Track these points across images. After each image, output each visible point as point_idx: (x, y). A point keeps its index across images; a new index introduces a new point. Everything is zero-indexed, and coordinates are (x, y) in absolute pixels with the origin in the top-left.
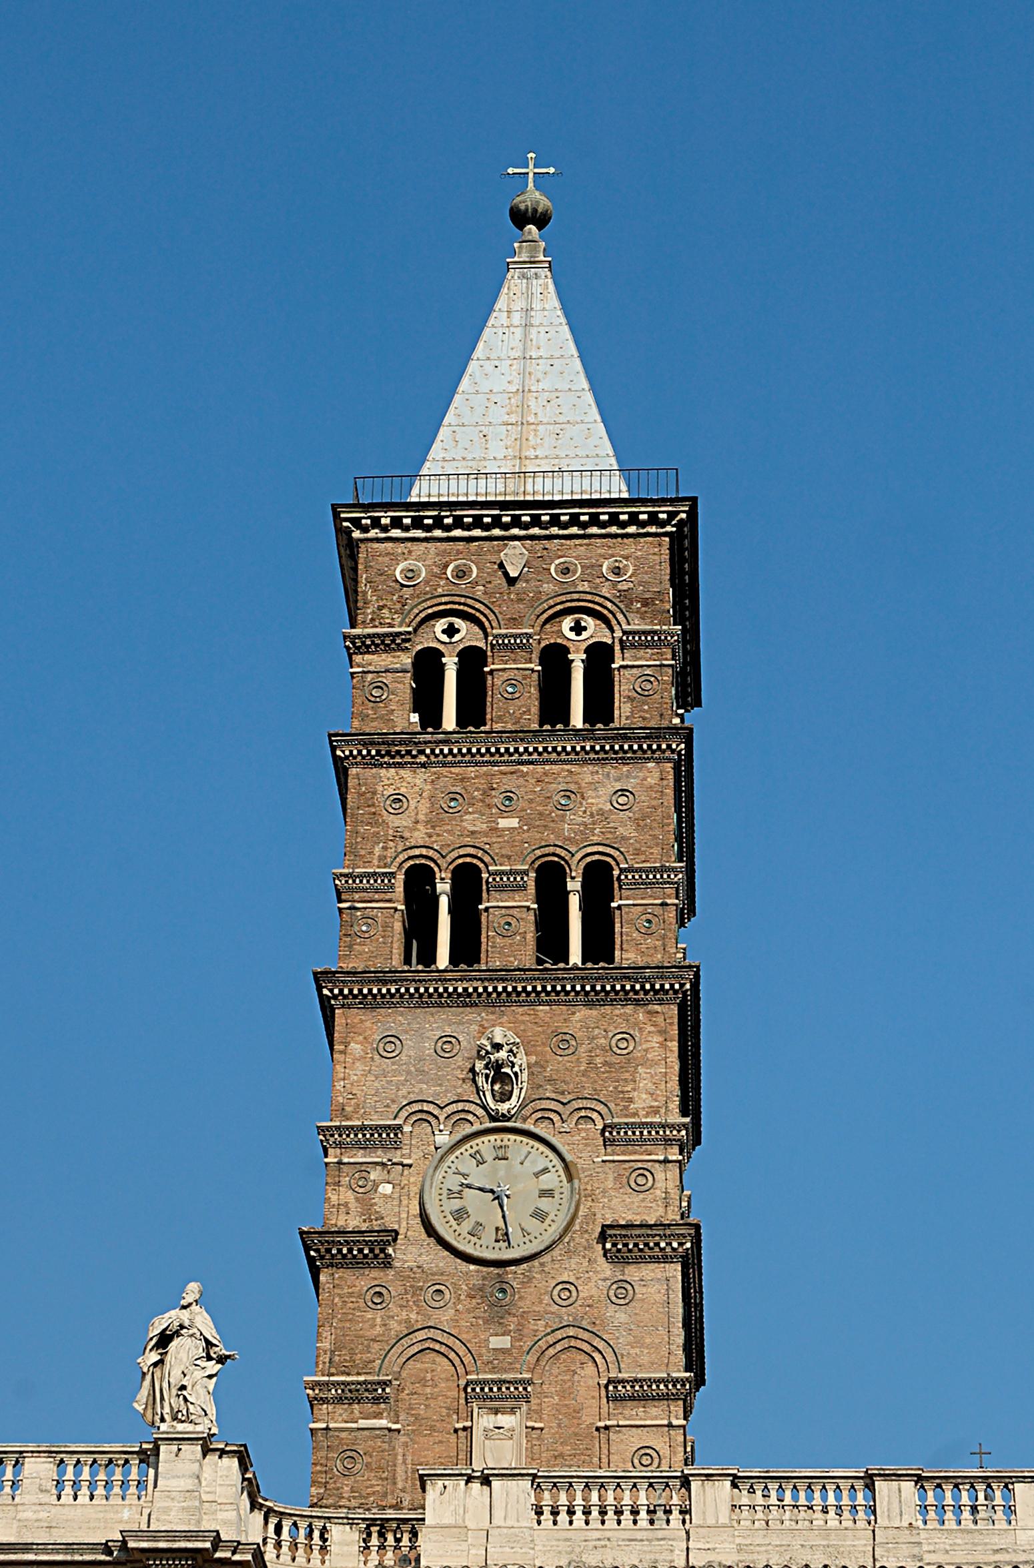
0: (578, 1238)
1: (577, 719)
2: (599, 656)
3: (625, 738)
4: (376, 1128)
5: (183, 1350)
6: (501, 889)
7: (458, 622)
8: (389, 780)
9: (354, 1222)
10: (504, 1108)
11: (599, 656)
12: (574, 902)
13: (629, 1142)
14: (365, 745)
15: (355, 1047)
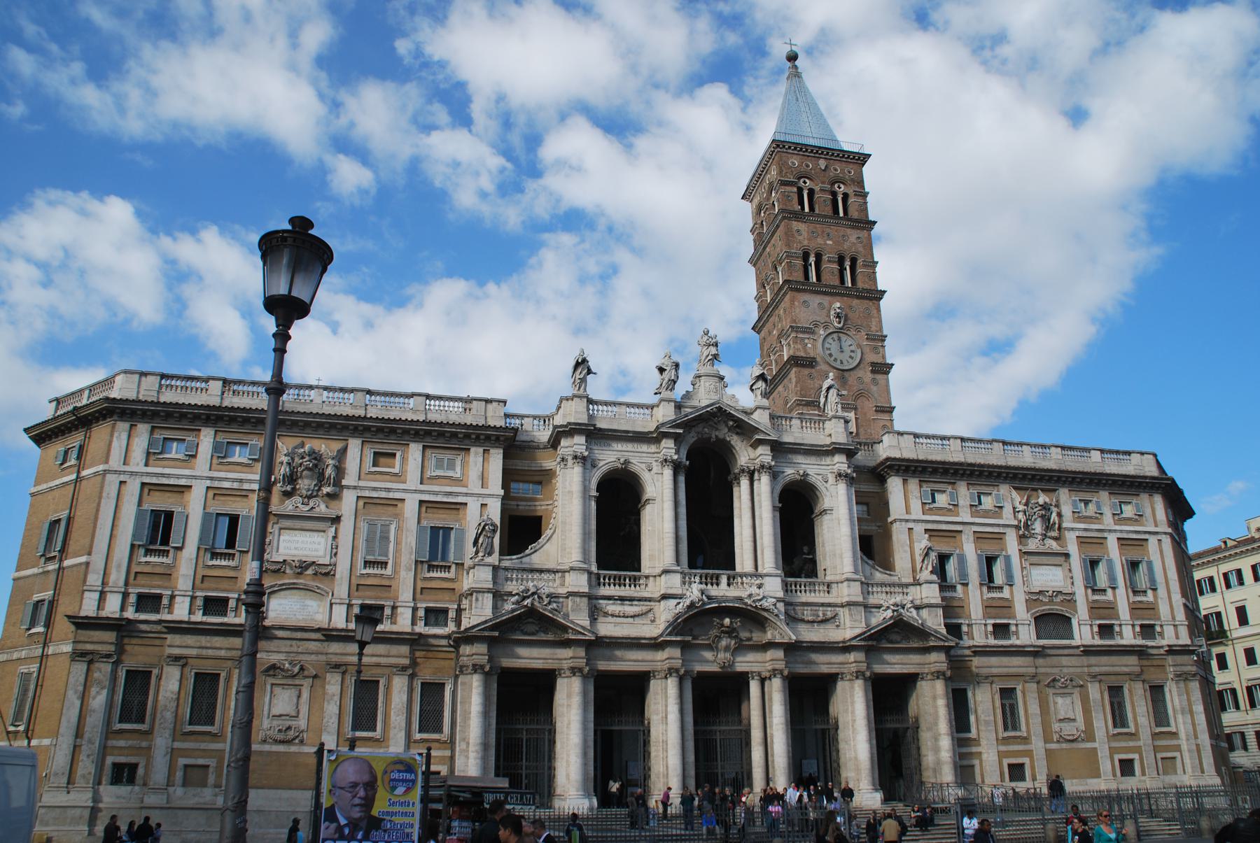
0: (862, 365)
1: (841, 214)
2: (846, 196)
3: (859, 222)
4: (806, 328)
5: (833, 392)
6: (829, 261)
7: (807, 180)
8: (796, 225)
9: (803, 354)
10: (840, 326)
11: (846, 196)
12: (848, 268)
13: (872, 339)
14: (790, 213)
15: (796, 303)
